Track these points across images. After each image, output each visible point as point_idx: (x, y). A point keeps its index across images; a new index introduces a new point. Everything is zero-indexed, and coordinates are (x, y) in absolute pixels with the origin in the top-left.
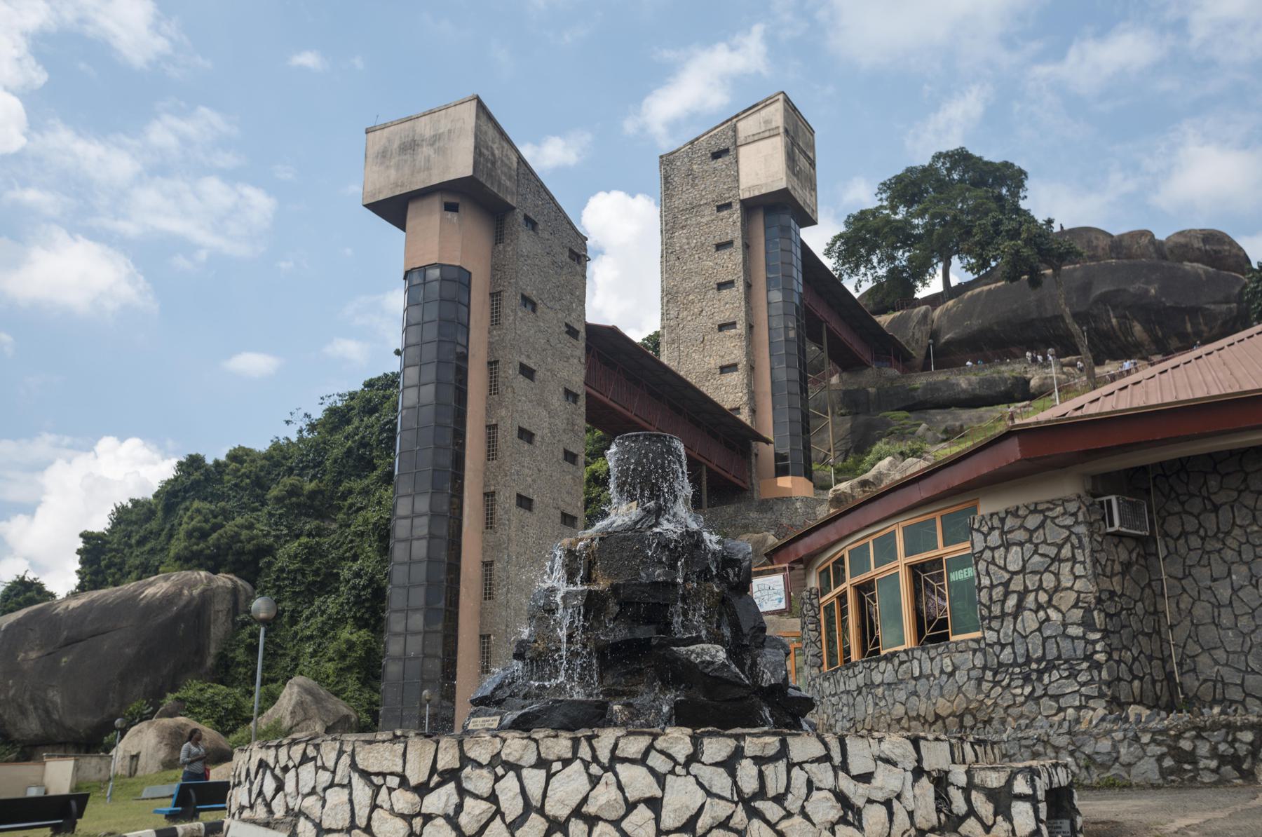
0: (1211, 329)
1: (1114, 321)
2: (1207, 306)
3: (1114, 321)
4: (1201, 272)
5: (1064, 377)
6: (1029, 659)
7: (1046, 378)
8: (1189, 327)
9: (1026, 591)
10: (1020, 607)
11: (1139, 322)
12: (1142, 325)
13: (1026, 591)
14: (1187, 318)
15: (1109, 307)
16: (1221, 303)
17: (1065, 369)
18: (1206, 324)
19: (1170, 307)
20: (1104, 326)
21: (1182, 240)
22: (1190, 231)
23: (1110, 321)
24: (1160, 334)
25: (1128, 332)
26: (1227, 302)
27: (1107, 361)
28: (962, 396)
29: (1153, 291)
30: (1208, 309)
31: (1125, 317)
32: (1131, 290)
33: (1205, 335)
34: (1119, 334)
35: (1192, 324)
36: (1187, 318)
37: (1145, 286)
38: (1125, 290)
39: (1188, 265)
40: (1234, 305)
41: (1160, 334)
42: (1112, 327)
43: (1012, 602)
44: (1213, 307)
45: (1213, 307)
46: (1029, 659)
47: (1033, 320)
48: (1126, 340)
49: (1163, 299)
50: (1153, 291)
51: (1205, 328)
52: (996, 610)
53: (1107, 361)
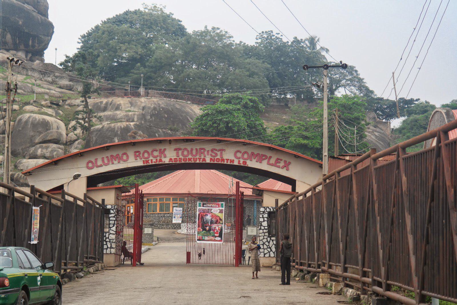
2: (40, 36)
4: (39, 18)
6: (190, 216)
9: (191, 209)
10: (190, 211)
12: (11, 35)
13: (191, 209)
14: (31, 38)
19: (27, 33)
24: (18, 42)
29: (21, 23)
31: (5, 30)
33: (36, 48)
39: (26, 6)
41: (18, 42)
43: (189, 210)
44: (43, 37)
45: (43, 37)
46: (190, 216)
49: (24, 28)
50: (21, 23)
51: (36, 45)
52: (187, 210)
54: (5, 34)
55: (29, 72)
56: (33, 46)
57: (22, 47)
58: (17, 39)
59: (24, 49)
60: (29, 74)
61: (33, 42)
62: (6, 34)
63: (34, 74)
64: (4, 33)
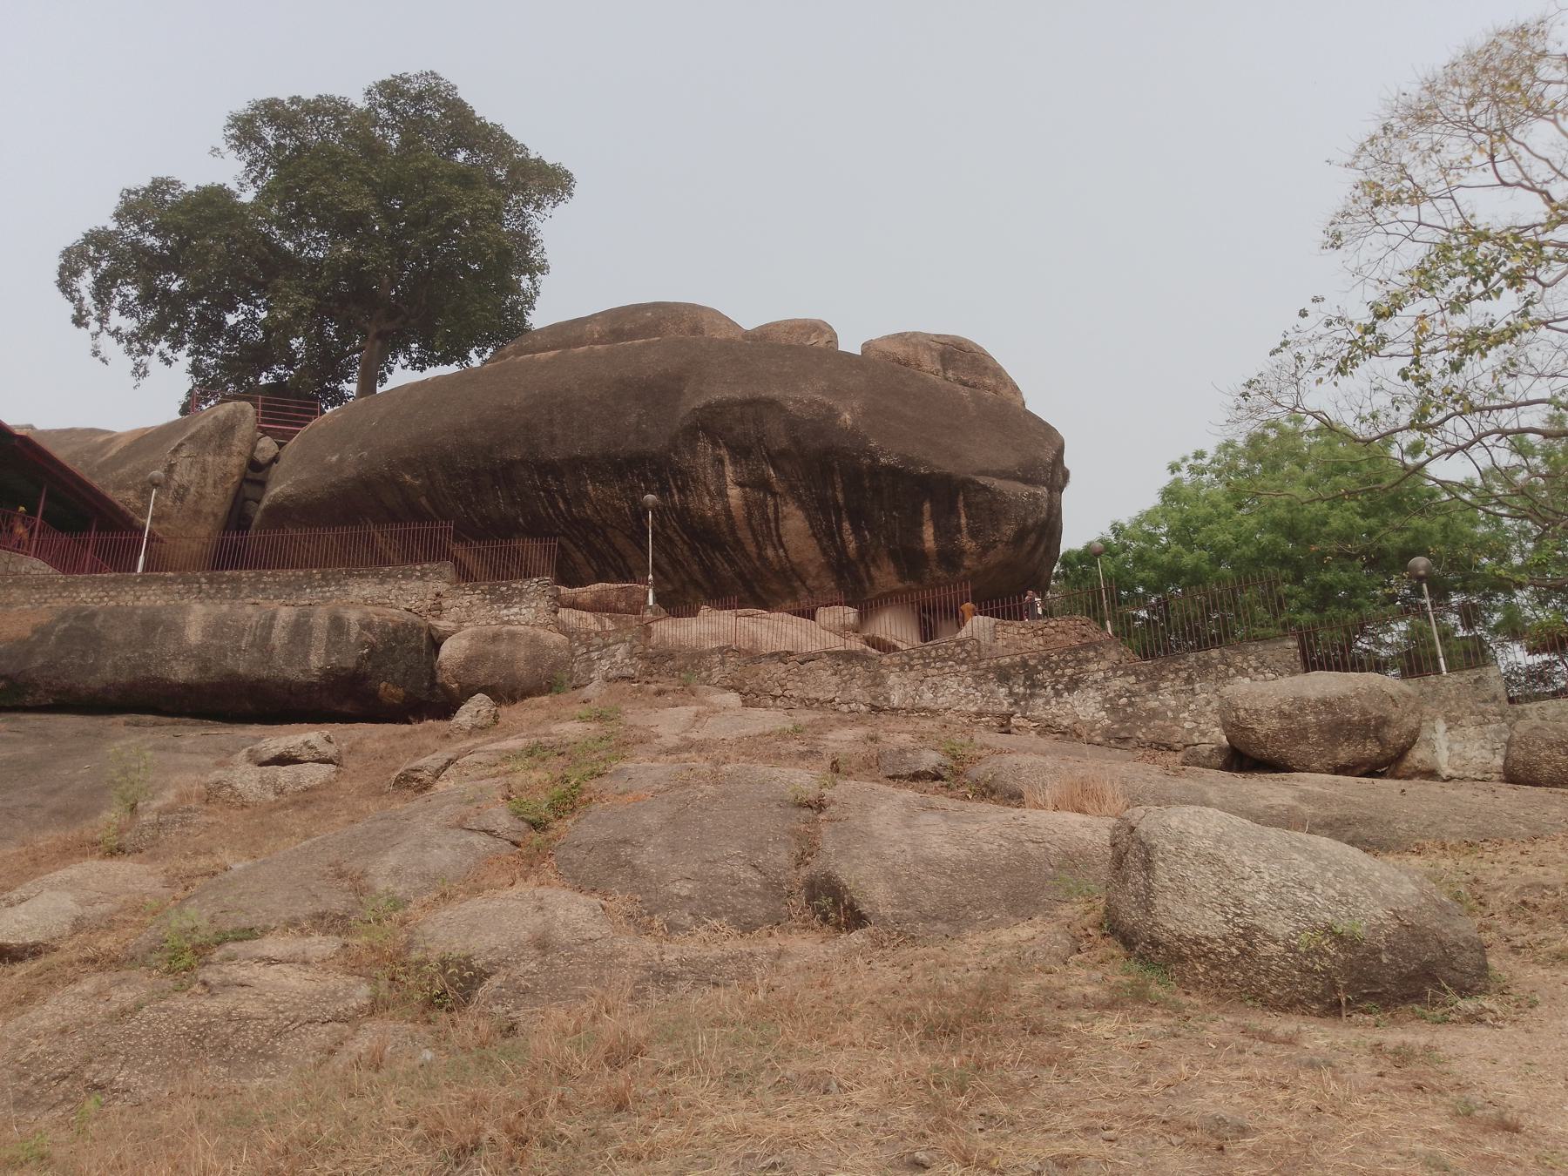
0: (985, 550)
1: (734, 492)
2: (982, 480)
3: (734, 492)
5: (558, 638)
7: (496, 638)
8: (928, 533)
11: (802, 506)
12: (809, 518)
14: (927, 506)
15: (723, 452)
16: (1017, 479)
17: (564, 614)
18: (974, 534)
19: (890, 470)
20: (706, 505)
21: (900, 351)
22: (915, 334)
23: (722, 493)
24: (852, 546)
25: (769, 529)
26: (1026, 481)
27: (704, 610)
28: (181, 672)
29: (847, 416)
30: (985, 488)
31: (764, 485)
32: (790, 405)
34: (744, 534)
35: (937, 527)
36: (927, 506)
37: (829, 401)
38: (772, 403)
40: (1042, 491)
41: (852, 546)
42: (727, 510)
45: (997, 484)
47: (512, 463)
48: (762, 557)
50: (847, 416)
51: (968, 543)
53: (704, 610)
54: (770, 511)
55: (892, 679)
56: (950, 557)
57: (886, 576)
58: (846, 525)
59: (900, 585)
60: (896, 700)
61: (946, 532)
62: (776, 512)
63: (935, 688)
64: (762, 505)
